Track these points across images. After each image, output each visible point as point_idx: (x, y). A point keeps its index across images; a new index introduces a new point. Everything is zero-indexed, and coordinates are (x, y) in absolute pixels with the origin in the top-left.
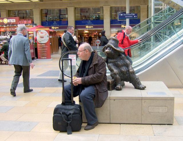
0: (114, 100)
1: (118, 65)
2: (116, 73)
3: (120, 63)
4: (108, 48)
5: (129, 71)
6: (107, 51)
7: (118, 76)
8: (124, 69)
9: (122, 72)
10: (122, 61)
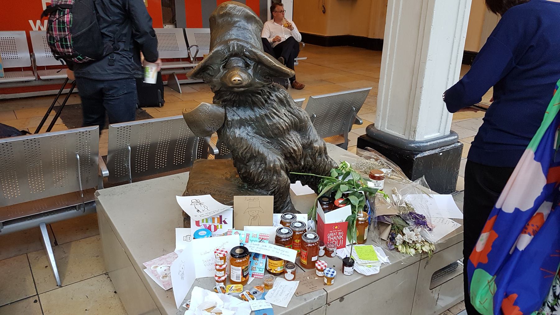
0: (342, 299)
1: (276, 131)
9: (289, 156)
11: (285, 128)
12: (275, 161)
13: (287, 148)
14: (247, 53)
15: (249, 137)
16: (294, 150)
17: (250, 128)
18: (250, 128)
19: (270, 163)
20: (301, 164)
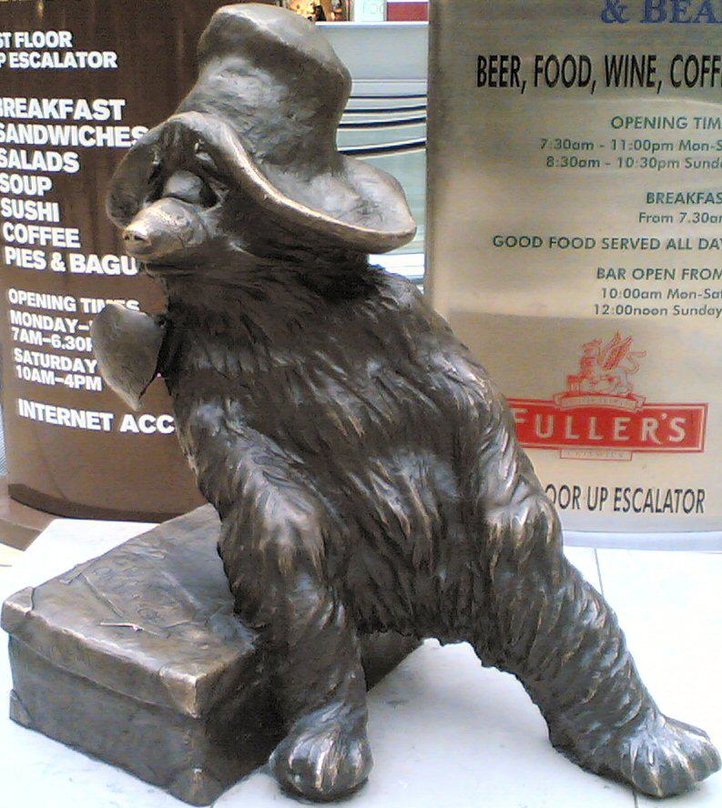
2: (285, 561)
3: (345, 402)
4: (180, 184)
5: (470, 512)
6: (153, 219)
7: (309, 598)
8: (404, 487)
10: (372, 366)
11: (359, 430)
12: (277, 530)
13: (365, 501)
14: (203, 157)
15: (224, 433)
16: (392, 516)
17: (236, 404)
18: (236, 404)
19: (259, 537)
20: (438, 580)
